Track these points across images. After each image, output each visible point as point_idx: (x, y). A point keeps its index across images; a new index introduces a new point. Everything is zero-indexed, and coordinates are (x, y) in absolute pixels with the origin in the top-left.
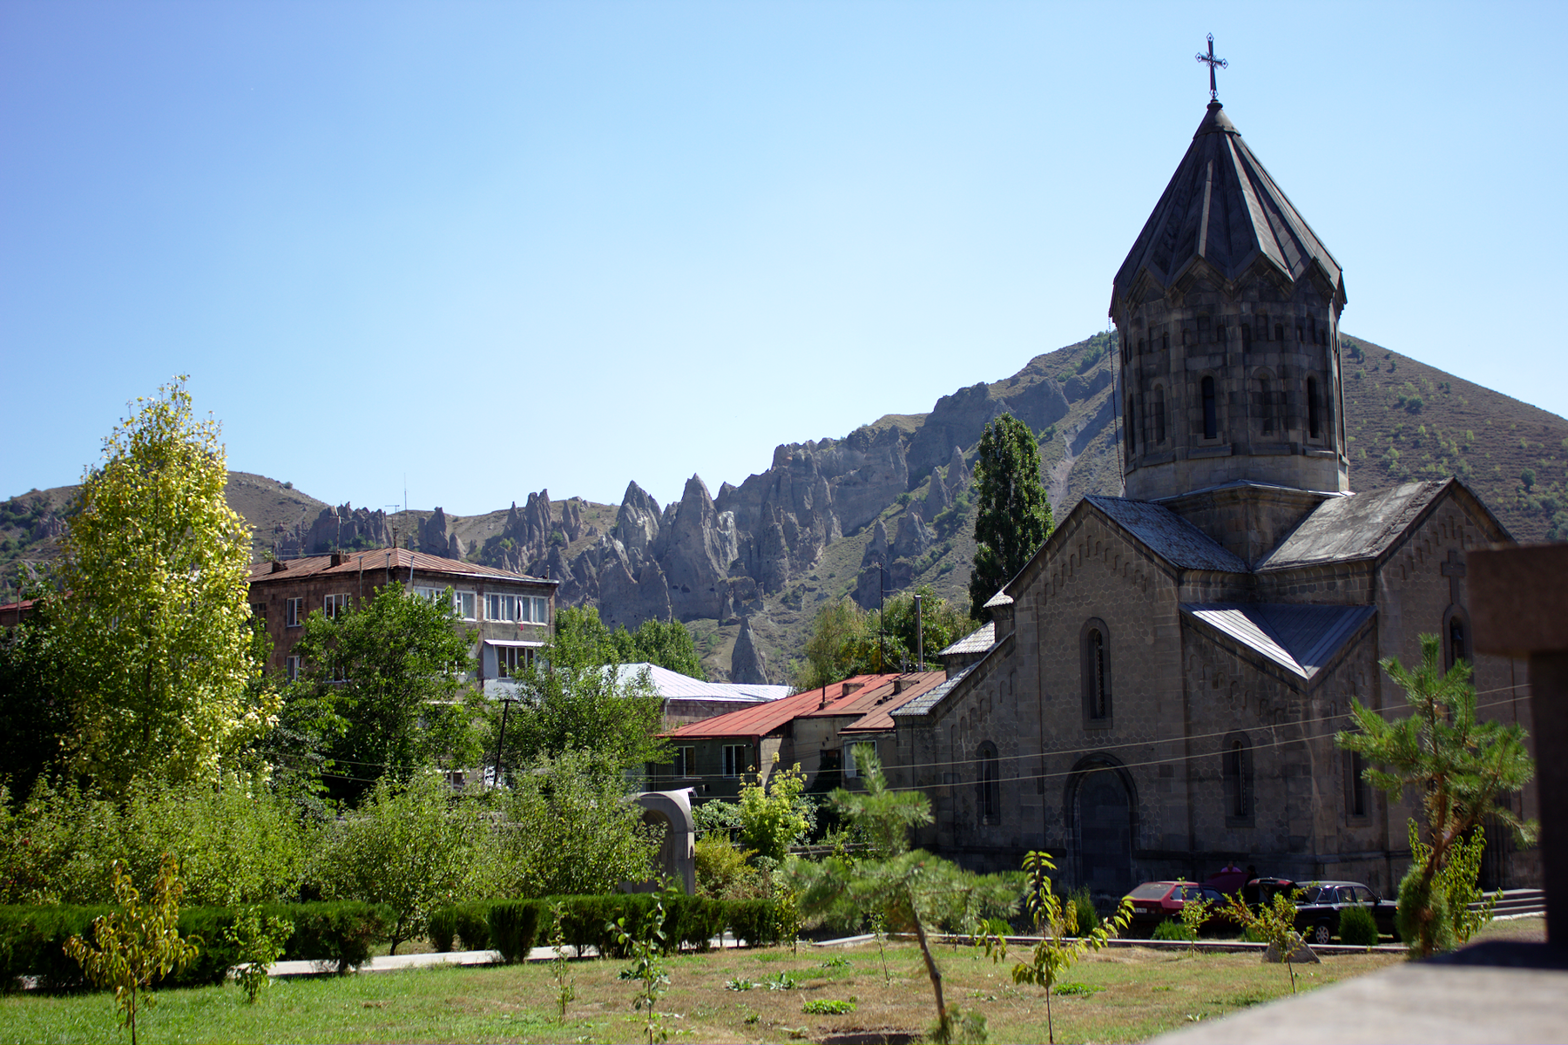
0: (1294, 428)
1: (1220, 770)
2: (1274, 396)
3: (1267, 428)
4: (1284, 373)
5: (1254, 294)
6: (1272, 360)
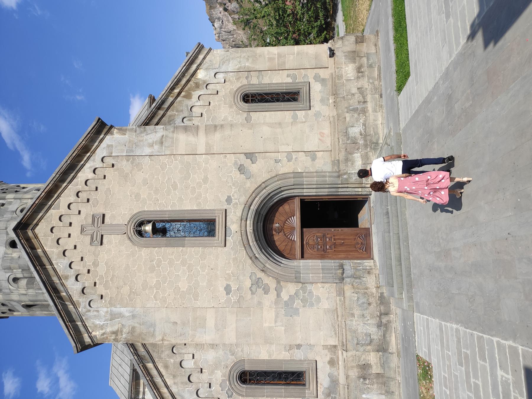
4: (10, 269)
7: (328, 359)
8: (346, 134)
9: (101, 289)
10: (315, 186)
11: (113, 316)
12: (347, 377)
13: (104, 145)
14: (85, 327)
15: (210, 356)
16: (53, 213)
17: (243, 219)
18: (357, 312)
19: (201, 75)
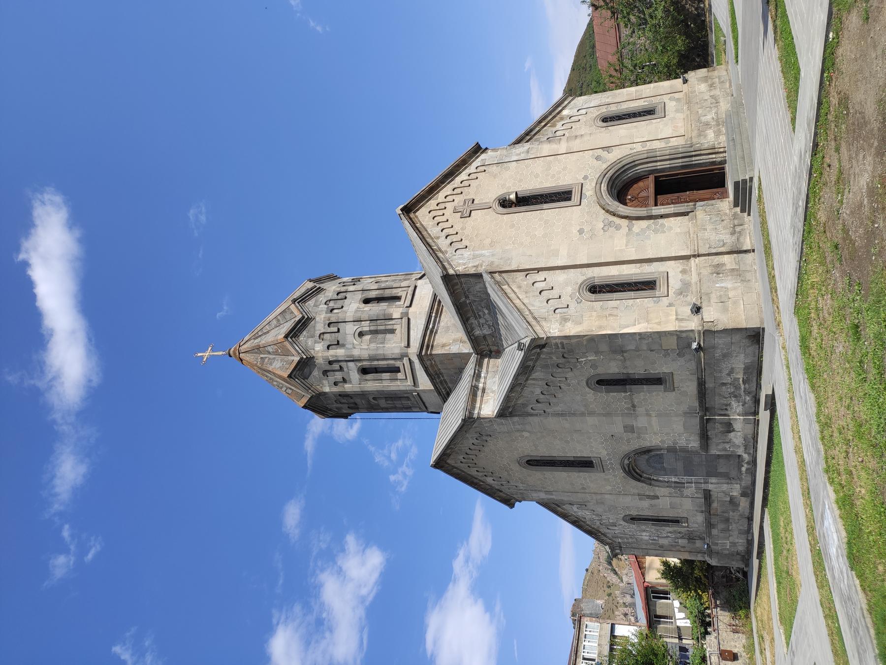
1: (623, 394)
2: (372, 328)
3: (392, 331)
5: (310, 342)
6: (350, 329)
7: (680, 269)
8: (699, 120)
9: (465, 242)
10: (667, 157)
12: (699, 274)
13: (479, 159)
14: (450, 264)
15: (560, 277)
16: (432, 204)
19: (565, 112)
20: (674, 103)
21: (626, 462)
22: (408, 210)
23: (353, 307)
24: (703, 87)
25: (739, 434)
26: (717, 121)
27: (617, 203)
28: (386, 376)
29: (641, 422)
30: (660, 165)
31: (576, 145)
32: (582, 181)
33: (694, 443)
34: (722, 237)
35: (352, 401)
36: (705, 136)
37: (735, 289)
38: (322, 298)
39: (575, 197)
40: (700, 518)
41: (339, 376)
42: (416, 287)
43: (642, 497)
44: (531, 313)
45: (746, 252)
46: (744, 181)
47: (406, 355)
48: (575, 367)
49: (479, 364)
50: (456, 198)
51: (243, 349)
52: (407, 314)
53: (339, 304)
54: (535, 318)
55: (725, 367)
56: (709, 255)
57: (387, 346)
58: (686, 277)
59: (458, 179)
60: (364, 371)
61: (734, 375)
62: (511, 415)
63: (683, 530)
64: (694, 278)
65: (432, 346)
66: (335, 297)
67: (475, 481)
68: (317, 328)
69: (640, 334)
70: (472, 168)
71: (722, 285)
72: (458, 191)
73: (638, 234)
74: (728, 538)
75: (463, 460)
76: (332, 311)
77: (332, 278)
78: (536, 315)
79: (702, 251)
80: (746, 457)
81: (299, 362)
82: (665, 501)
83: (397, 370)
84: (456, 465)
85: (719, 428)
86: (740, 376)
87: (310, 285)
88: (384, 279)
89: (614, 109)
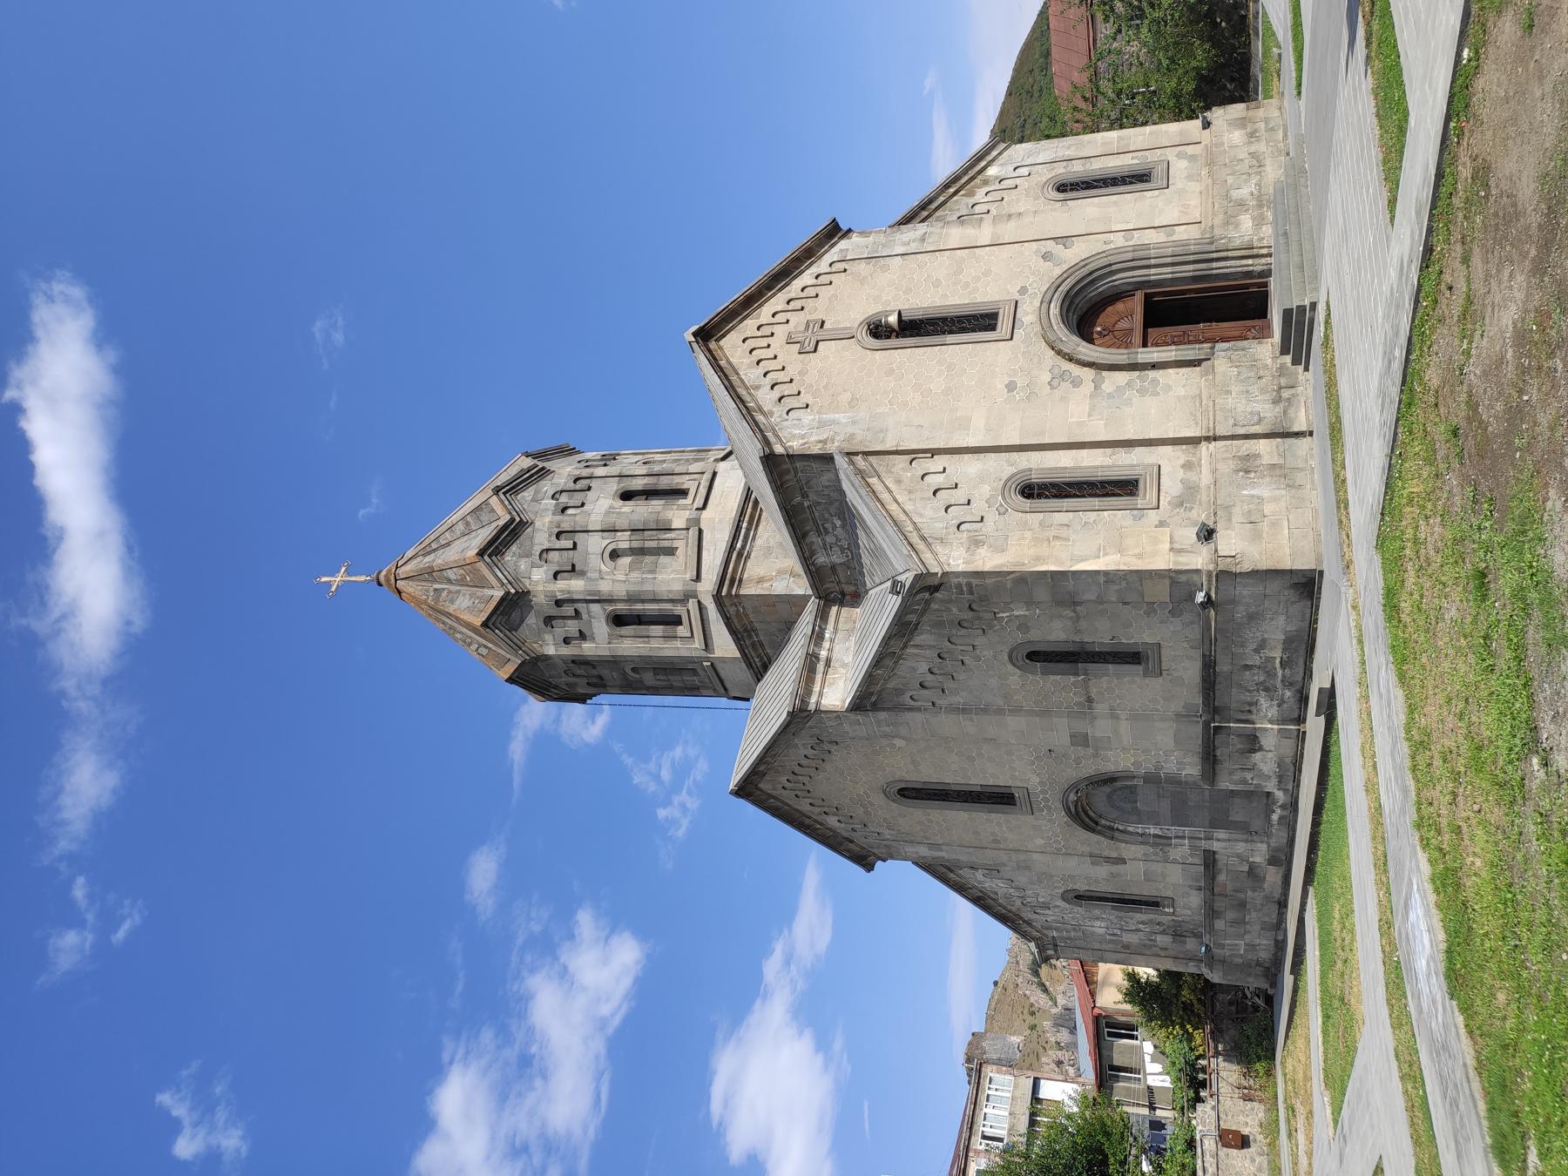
0: (670, 521)
1: (1072, 679)
2: (635, 544)
3: (671, 552)
5: (523, 565)
6: (595, 545)
7: (1182, 461)
8: (1227, 197)
9: (805, 398)
10: (1169, 260)
11: (822, 425)
12: (1214, 471)
14: (777, 436)
15: (969, 467)
16: (749, 326)
17: (1046, 302)
18: (1235, 389)
19: (992, 171)
20: (1183, 164)
21: (1072, 797)
22: (706, 335)
23: (602, 505)
24: (1237, 136)
25: (1270, 755)
26: (1259, 198)
27: (1076, 339)
28: (657, 630)
29: (1101, 728)
30: (1155, 274)
31: (1009, 231)
32: (1017, 297)
33: (1191, 769)
34: (1258, 407)
35: (595, 672)
36: (1237, 226)
37: (1275, 499)
38: (547, 486)
39: (1004, 325)
40: (1195, 900)
41: (572, 627)
42: (715, 474)
43: (1096, 859)
44: (917, 529)
45: (1298, 435)
46: (1301, 309)
47: (694, 595)
48: (991, 627)
49: (822, 615)
50: (792, 317)
51: (402, 572)
52: (697, 521)
53: (577, 499)
54: (924, 539)
55: (1252, 636)
56: (1233, 437)
57: (660, 577)
58: (1192, 476)
59: (797, 284)
60: (618, 620)
61: (1267, 653)
62: (875, 707)
63: (1164, 919)
64: (1205, 478)
65: (741, 580)
66: (571, 486)
67: (807, 821)
68: (536, 540)
69: (1106, 573)
70: (822, 265)
71: (1253, 492)
72: (796, 305)
73: (1110, 396)
74: (1241, 937)
75: (788, 785)
76: (564, 510)
77: (566, 451)
78: (926, 533)
79: (1221, 431)
80: (1280, 795)
81: (502, 600)
82: (1137, 868)
83: (676, 621)
84: (775, 793)
85: (1236, 743)
86: (1277, 654)
87: (527, 463)
88: (658, 457)
89: (1078, 170)
